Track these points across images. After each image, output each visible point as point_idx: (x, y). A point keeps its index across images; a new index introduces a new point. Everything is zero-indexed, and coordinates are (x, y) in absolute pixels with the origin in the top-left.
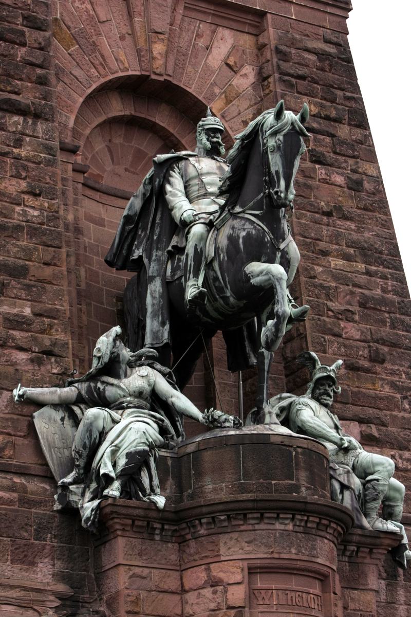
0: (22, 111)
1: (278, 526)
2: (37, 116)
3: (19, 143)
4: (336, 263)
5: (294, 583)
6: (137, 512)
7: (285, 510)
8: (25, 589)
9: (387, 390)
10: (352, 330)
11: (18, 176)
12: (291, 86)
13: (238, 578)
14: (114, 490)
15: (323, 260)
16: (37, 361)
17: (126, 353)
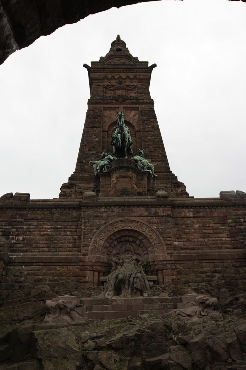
0: (96, 127)
1: (120, 171)
2: (98, 127)
3: (95, 131)
4: (148, 138)
5: (124, 179)
6: (101, 173)
7: (121, 168)
8: (87, 187)
9: (157, 154)
10: (151, 147)
11: (95, 135)
12: (142, 115)
13: (115, 179)
14: (99, 171)
15: (146, 138)
16: (95, 158)
17: (106, 154)
